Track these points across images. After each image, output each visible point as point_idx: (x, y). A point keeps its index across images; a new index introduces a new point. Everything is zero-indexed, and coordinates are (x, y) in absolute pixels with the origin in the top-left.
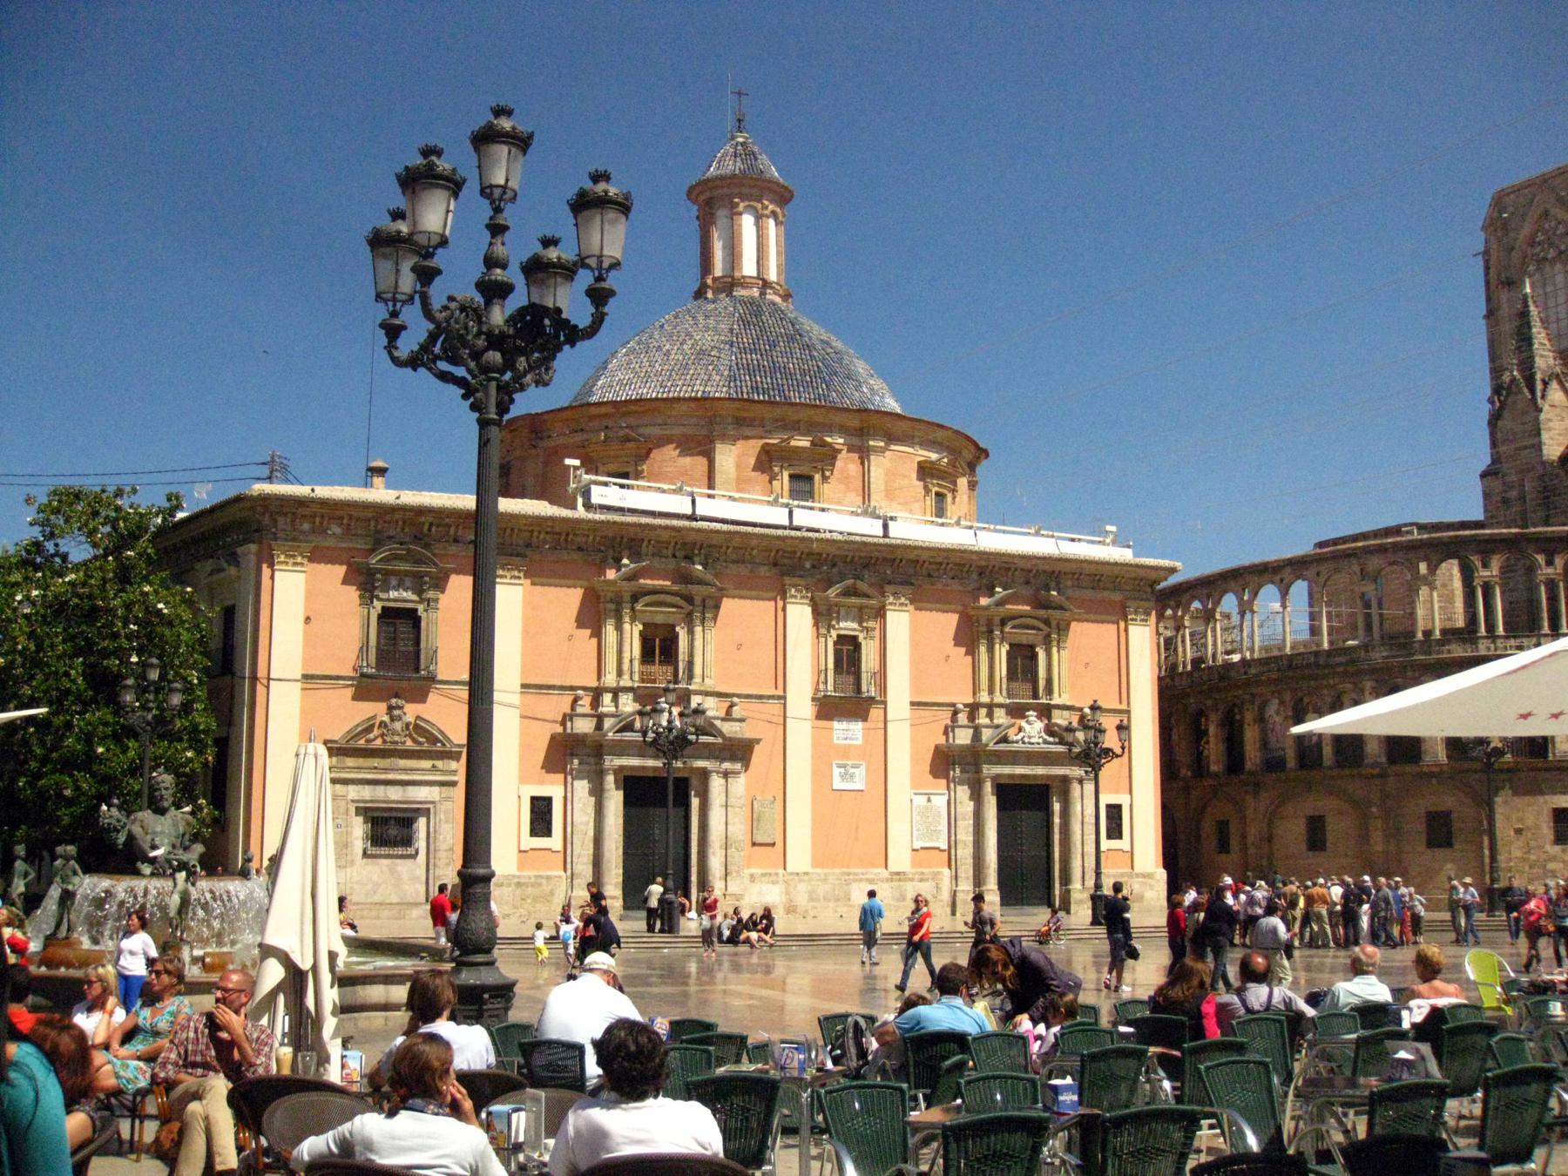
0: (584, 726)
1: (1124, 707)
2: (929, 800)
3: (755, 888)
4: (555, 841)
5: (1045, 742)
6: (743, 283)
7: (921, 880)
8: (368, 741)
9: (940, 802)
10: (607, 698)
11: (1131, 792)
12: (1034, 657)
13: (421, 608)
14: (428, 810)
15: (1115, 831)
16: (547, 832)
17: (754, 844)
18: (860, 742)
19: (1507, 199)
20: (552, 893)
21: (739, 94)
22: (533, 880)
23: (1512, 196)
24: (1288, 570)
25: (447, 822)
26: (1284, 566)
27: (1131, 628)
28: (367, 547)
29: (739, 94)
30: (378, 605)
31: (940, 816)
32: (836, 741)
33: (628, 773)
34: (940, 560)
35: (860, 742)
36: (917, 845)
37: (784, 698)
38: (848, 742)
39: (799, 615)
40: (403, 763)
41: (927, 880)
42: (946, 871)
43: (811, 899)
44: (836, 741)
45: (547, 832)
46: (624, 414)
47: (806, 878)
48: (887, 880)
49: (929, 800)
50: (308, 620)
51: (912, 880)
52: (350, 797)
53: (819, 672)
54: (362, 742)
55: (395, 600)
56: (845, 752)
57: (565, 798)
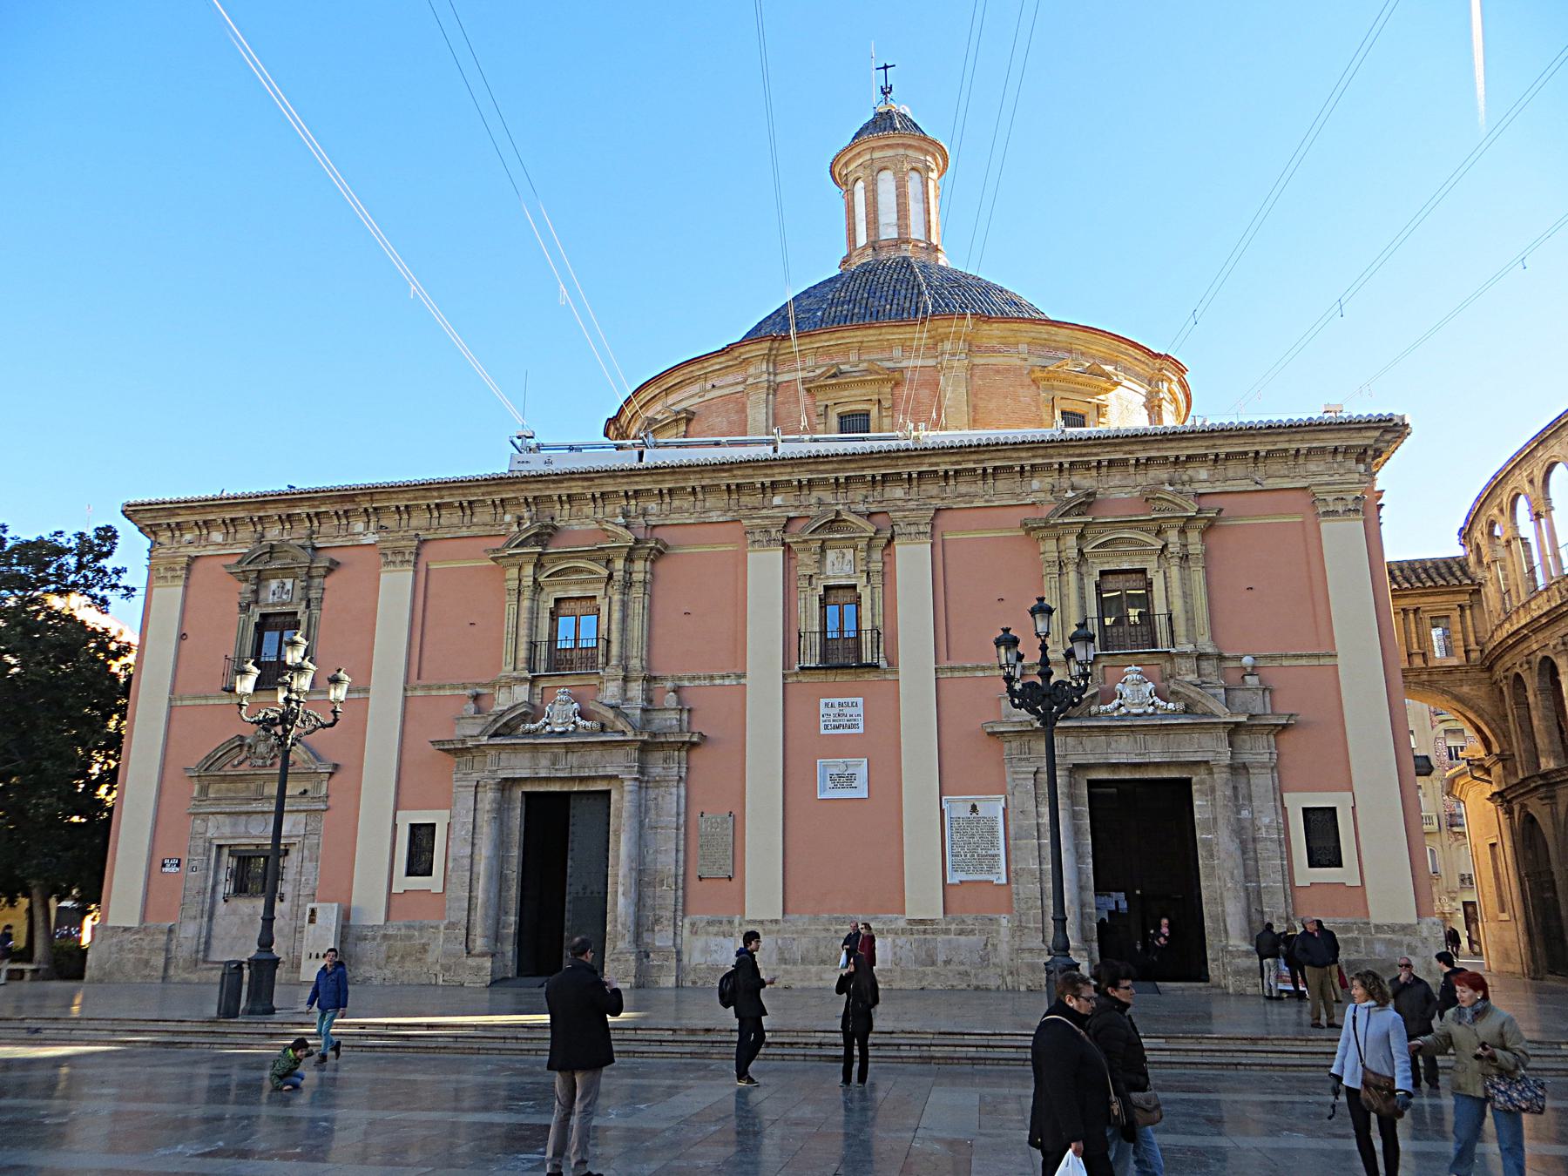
2: (974, 809)
3: (699, 942)
7: (961, 933)
8: (234, 766)
11: (1351, 789)
12: (1149, 585)
15: (1324, 850)
18: (861, 730)
20: (424, 949)
21: (886, 67)
22: (403, 931)
25: (310, 861)
28: (246, 551)
31: (992, 831)
32: (823, 731)
33: (528, 789)
34: (971, 465)
35: (861, 730)
37: (744, 676)
38: (841, 731)
39: (765, 566)
41: (972, 932)
43: (784, 961)
44: (823, 731)
47: (775, 927)
48: (903, 931)
49: (974, 809)
50: (183, 636)
51: (947, 932)
52: (209, 835)
54: (228, 767)
55: (274, 605)
56: (839, 747)
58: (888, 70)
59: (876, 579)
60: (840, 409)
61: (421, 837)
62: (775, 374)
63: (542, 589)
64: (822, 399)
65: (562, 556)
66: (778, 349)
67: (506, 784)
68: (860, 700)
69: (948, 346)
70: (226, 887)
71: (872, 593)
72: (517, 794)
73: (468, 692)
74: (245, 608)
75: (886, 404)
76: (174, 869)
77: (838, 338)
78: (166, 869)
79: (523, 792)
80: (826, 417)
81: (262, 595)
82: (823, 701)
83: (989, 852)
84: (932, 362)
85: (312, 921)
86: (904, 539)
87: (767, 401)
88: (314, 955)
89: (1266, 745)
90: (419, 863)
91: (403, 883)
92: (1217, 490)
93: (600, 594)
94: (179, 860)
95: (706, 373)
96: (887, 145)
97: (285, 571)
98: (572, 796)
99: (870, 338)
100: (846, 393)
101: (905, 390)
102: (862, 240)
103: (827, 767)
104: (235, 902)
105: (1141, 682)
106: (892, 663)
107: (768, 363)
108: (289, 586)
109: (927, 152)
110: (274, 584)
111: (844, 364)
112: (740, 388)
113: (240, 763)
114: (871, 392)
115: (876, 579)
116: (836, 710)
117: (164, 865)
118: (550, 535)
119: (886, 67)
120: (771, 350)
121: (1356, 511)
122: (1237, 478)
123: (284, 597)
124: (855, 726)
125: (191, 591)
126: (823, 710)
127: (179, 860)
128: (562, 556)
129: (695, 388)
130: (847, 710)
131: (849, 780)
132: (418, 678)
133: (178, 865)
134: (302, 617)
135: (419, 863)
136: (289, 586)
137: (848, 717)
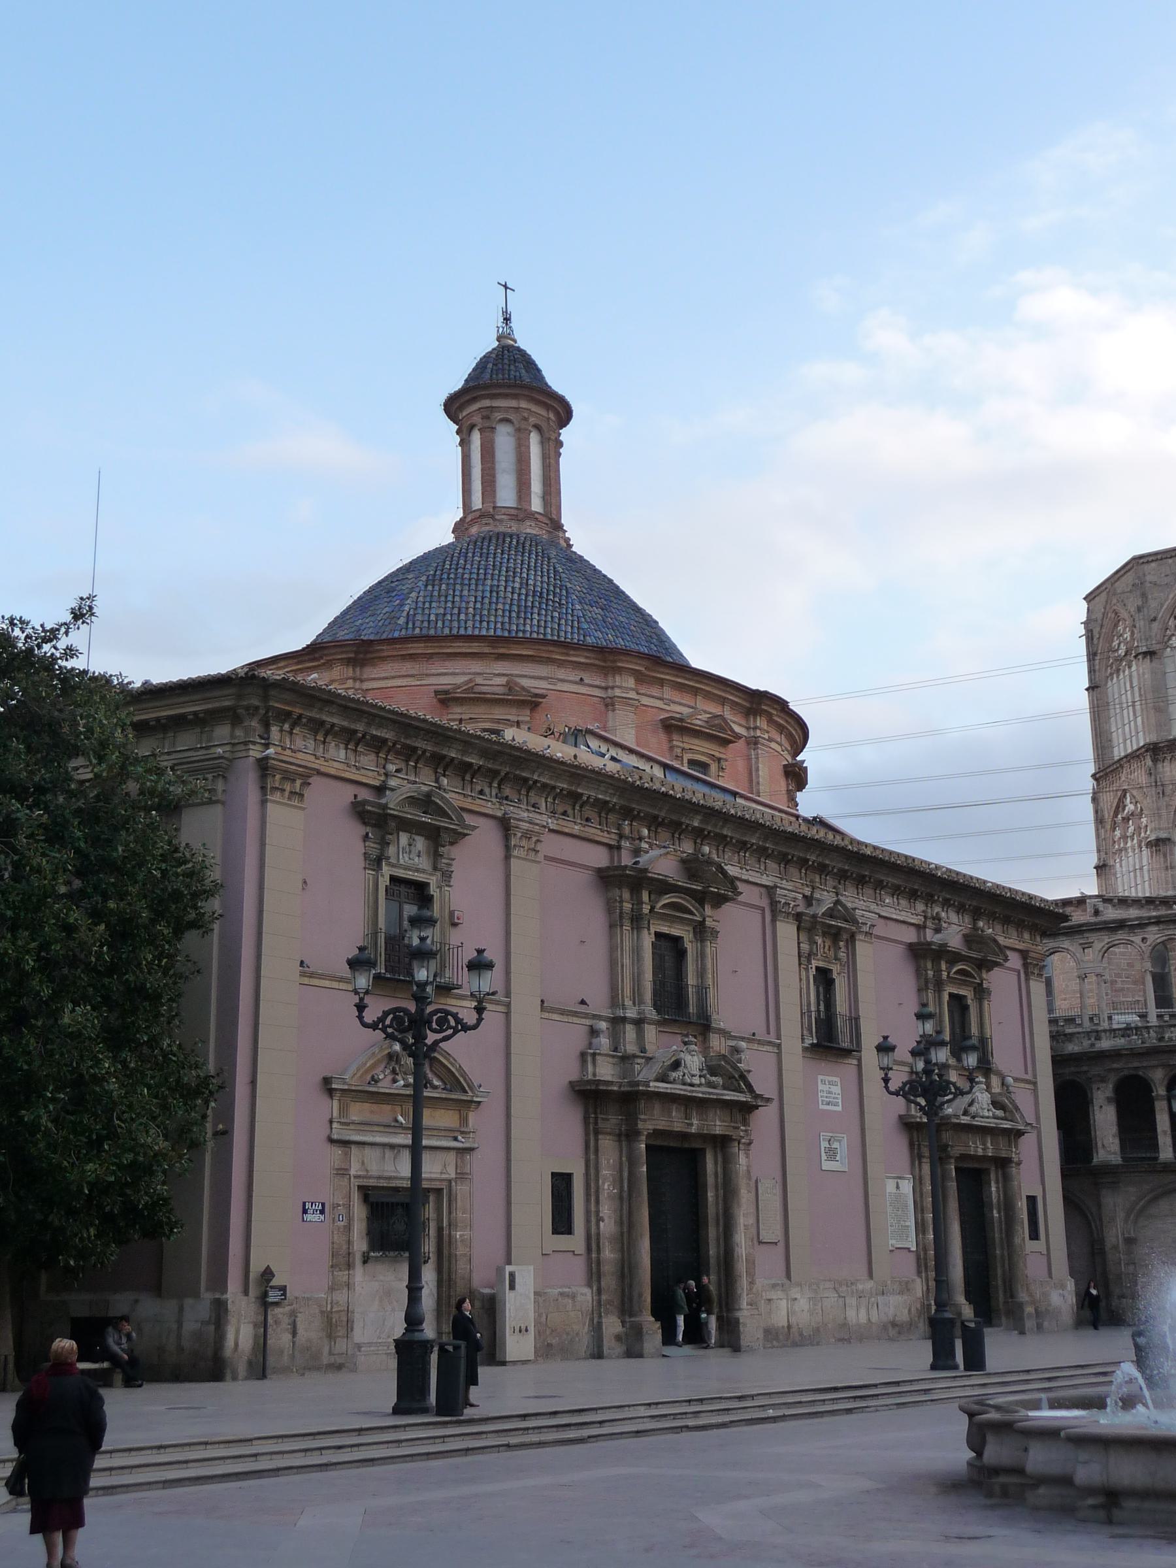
0: (606, 1071)
1: (1029, 1077)
4: (576, 1241)
5: (995, 1117)
6: (531, 516)
10: (630, 1031)
13: (433, 881)
14: (439, 1191)
17: (760, 1242)
18: (839, 1108)
19: (1146, 567)
23: (1153, 565)
24: (1154, 928)
26: (1147, 925)
27: (1032, 983)
29: (506, 287)
32: (821, 1107)
35: (839, 1108)
42: (918, 1281)
44: (821, 1107)
46: (502, 657)
53: (802, 1014)
55: (407, 868)
57: (587, 1174)
70: (360, 1244)
73: (588, 1022)
76: (317, 1217)
78: (308, 1217)
82: (820, 1077)
85: (512, 1287)
88: (517, 1330)
94: (323, 1205)
102: (506, 496)
117: (305, 1211)
123: (416, 859)
124: (836, 1105)
126: (821, 1087)
127: (323, 1205)
131: (832, 1154)
133: (322, 1212)
135: (562, 1223)
137: (833, 1096)
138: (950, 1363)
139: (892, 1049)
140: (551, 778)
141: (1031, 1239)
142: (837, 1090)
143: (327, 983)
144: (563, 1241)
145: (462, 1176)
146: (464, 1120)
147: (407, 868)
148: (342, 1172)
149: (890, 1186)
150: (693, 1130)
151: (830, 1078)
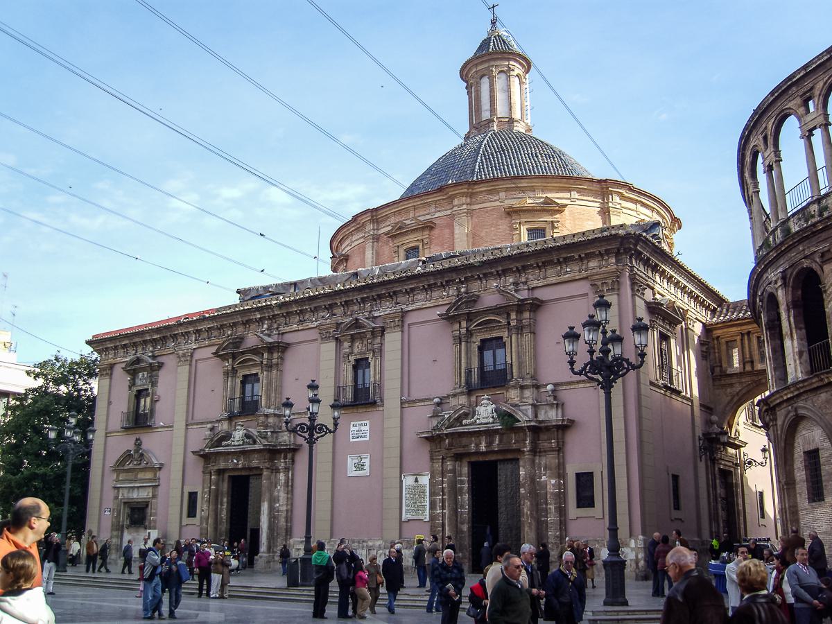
2: (416, 480)
9: (425, 480)
16: (194, 516)
18: (368, 439)
21: (493, 7)
30: (135, 389)
31: (424, 492)
32: (351, 440)
33: (232, 474)
35: (368, 439)
36: (405, 517)
40: (141, 476)
44: (351, 440)
45: (194, 516)
49: (416, 480)
55: (140, 386)
58: (495, 8)
59: (378, 354)
60: (405, 247)
61: (193, 496)
62: (378, 230)
63: (237, 371)
64: (399, 241)
65: (243, 353)
66: (376, 216)
67: (220, 472)
68: (368, 422)
69: (456, 202)
70: (127, 522)
71: (375, 362)
72: (226, 476)
74: (130, 388)
75: (425, 241)
76: (109, 513)
77: (402, 206)
78: (106, 513)
79: (229, 476)
80: (398, 251)
81: (137, 380)
82: (352, 423)
83: (422, 504)
84: (448, 212)
86: (389, 330)
87: (373, 247)
89: (556, 437)
90: (192, 512)
91: (186, 521)
92: (540, 285)
93: (259, 372)
95: (351, 232)
96: (483, 61)
97: (143, 369)
98: (251, 477)
99: (419, 203)
100: (407, 237)
101: (436, 232)
103: (351, 462)
104: (130, 529)
105: (488, 404)
106: (382, 400)
107: (373, 223)
108: (146, 376)
109: (509, 60)
110: (140, 375)
111: (408, 219)
112: (362, 240)
113: (129, 464)
114: (417, 236)
115: (378, 354)
116: (357, 428)
118: (241, 342)
119: (493, 7)
120: (372, 216)
121: (613, 289)
122: (552, 275)
124: (365, 437)
125: (113, 380)
126: (352, 428)
128: (243, 353)
129: (347, 242)
130: (362, 428)
132: (192, 419)
134: (150, 391)
136: (146, 376)
138: (620, 599)
139: (318, 401)
140: (185, 329)
141: (580, 504)
142: (367, 428)
143: (115, 434)
144: (191, 521)
145: (154, 496)
146: (155, 475)
147: (140, 386)
148: (117, 498)
149: (409, 481)
150: (240, 466)
151: (360, 422)
